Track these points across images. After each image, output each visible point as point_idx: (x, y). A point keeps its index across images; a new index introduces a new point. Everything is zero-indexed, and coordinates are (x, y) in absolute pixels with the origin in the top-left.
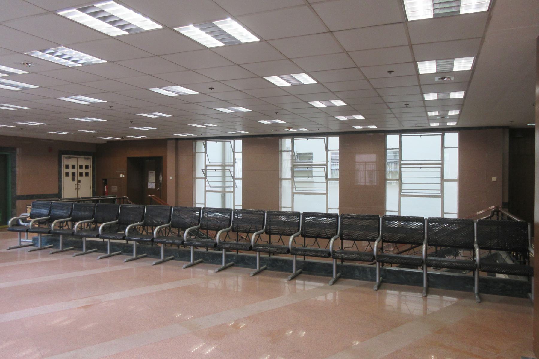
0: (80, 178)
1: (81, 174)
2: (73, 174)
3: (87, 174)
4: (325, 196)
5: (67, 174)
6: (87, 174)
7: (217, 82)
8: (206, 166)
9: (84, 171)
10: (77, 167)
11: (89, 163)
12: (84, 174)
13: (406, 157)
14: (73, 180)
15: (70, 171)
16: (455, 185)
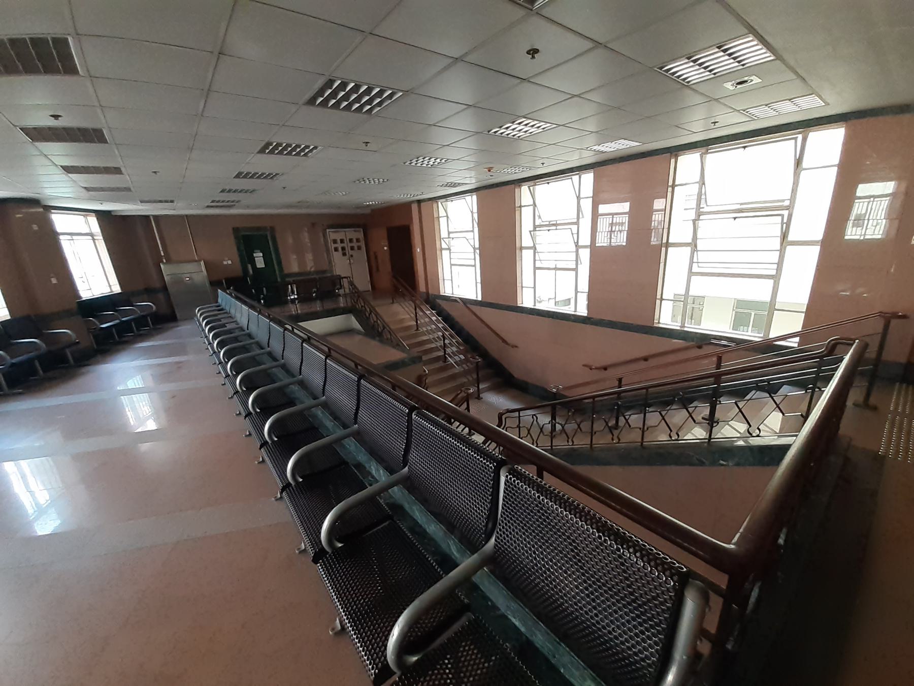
0: (351, 252)
1: (352, 248)
2: (343, 249)
3: (359, 248)
4: (574, 273)
5: (336, 249)
6: (359, 248)
7: (575, 99)
8: (449, 233)
9: (355, 245)
10: (347, 241)
11: (361, 235)
12: (356, 248)
13: (715, 198)
14: (344, 254)
15: (339, 246)
16: (814, 252)
